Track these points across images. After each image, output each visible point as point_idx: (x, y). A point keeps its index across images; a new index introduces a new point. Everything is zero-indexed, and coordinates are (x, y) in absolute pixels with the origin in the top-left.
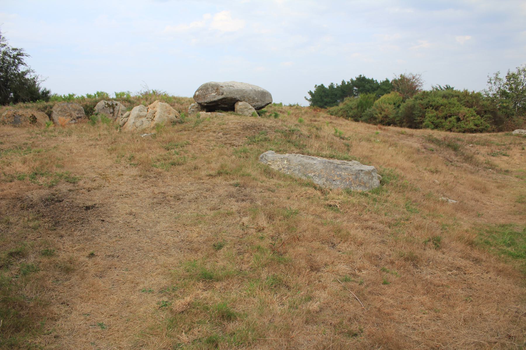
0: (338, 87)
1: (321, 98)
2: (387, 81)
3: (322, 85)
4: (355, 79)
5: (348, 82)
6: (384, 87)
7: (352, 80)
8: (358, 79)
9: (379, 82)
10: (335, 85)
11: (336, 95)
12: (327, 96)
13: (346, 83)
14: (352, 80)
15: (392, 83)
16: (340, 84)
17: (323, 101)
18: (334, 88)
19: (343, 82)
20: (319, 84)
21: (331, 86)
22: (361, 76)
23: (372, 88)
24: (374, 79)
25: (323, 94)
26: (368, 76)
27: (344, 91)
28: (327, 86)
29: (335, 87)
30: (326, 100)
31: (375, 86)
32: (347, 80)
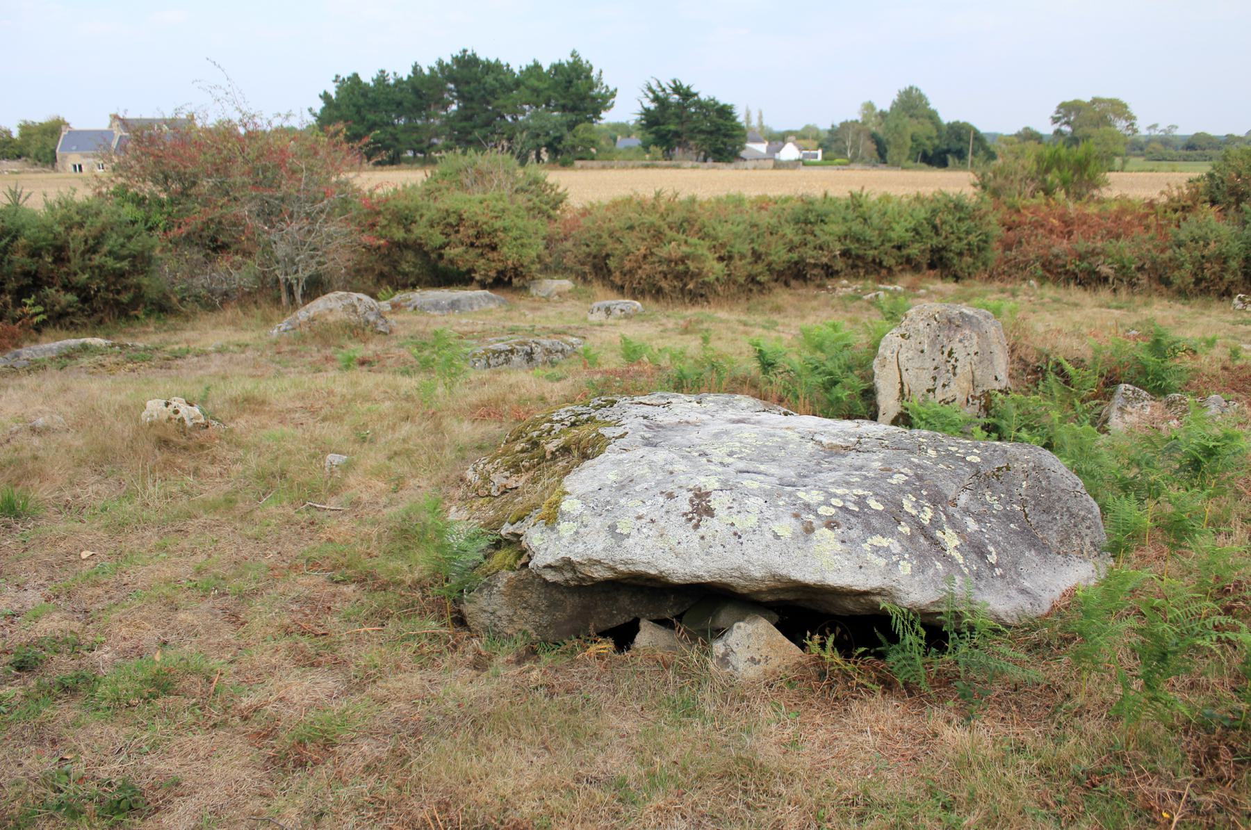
0: (399, 82)
1: (358, 112)
2: (537, 67)
3: (356, 75)
4: (448, 60)
5: (431, 69)
6: (534, 82)
7: (440, 63)
8: (456, 60)
9: (517, 71)
10: (391, 75)
11: (399, 104)
12: (374, 105)
13: (426, 72)
14: (440, 63)
15: (549, 71)
16: (405, 73)
17: (363, 119)
18: (388, 85)
19: (416, 70)
20: (346, 74)
21: (381, 79)
22: (465, 51)
23: (503, 84)
24: (503, 62)
25: (362, 101)
26: (485, 54)
27: (420, 92)
28: (367, 78)
29: (392, 81)
30: (371, 117)
31: (509, 80)
32: (428, 64)
